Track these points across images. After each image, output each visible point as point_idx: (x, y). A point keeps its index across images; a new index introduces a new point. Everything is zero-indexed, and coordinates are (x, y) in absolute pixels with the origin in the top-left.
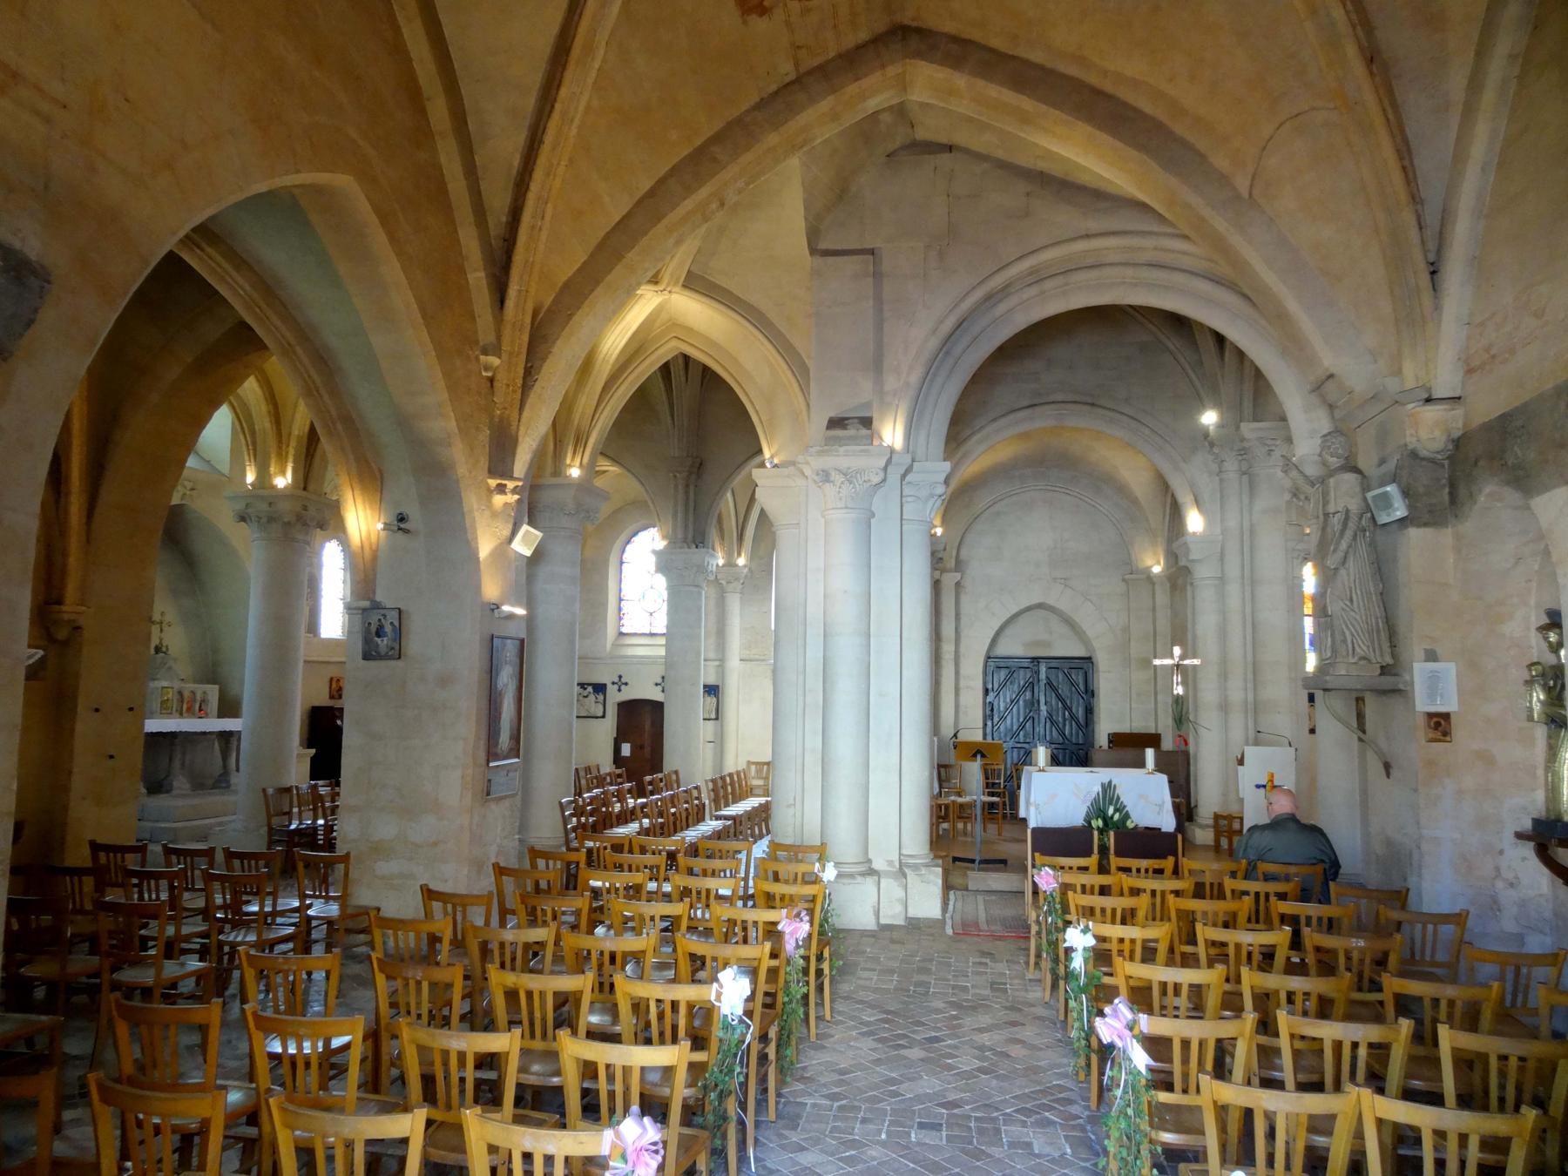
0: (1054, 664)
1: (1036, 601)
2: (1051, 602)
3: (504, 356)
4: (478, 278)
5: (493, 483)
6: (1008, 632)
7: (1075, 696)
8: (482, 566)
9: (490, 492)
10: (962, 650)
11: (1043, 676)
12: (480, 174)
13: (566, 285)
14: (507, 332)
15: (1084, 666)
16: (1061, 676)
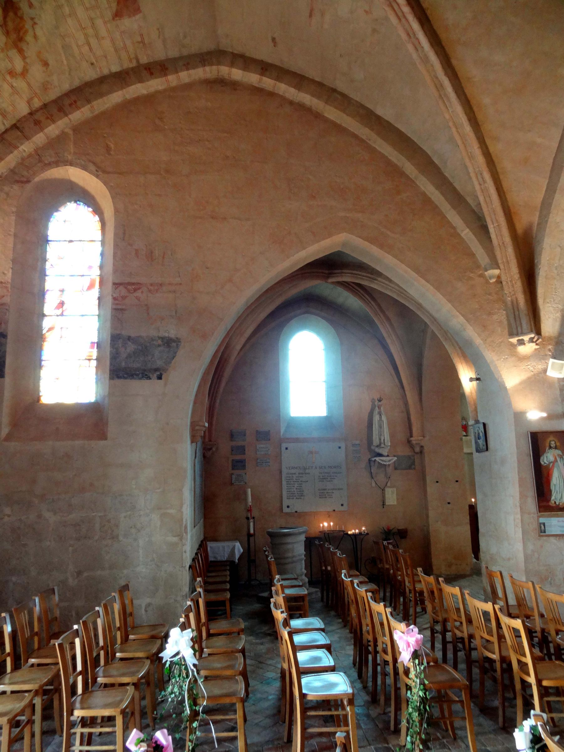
3: (502, 266)
4: (466, 234)
5: (514, 340)
8: (510, 392)
9: (513, 346)
12: (451, 180)
13: (543, 203)
14: (498, 253)
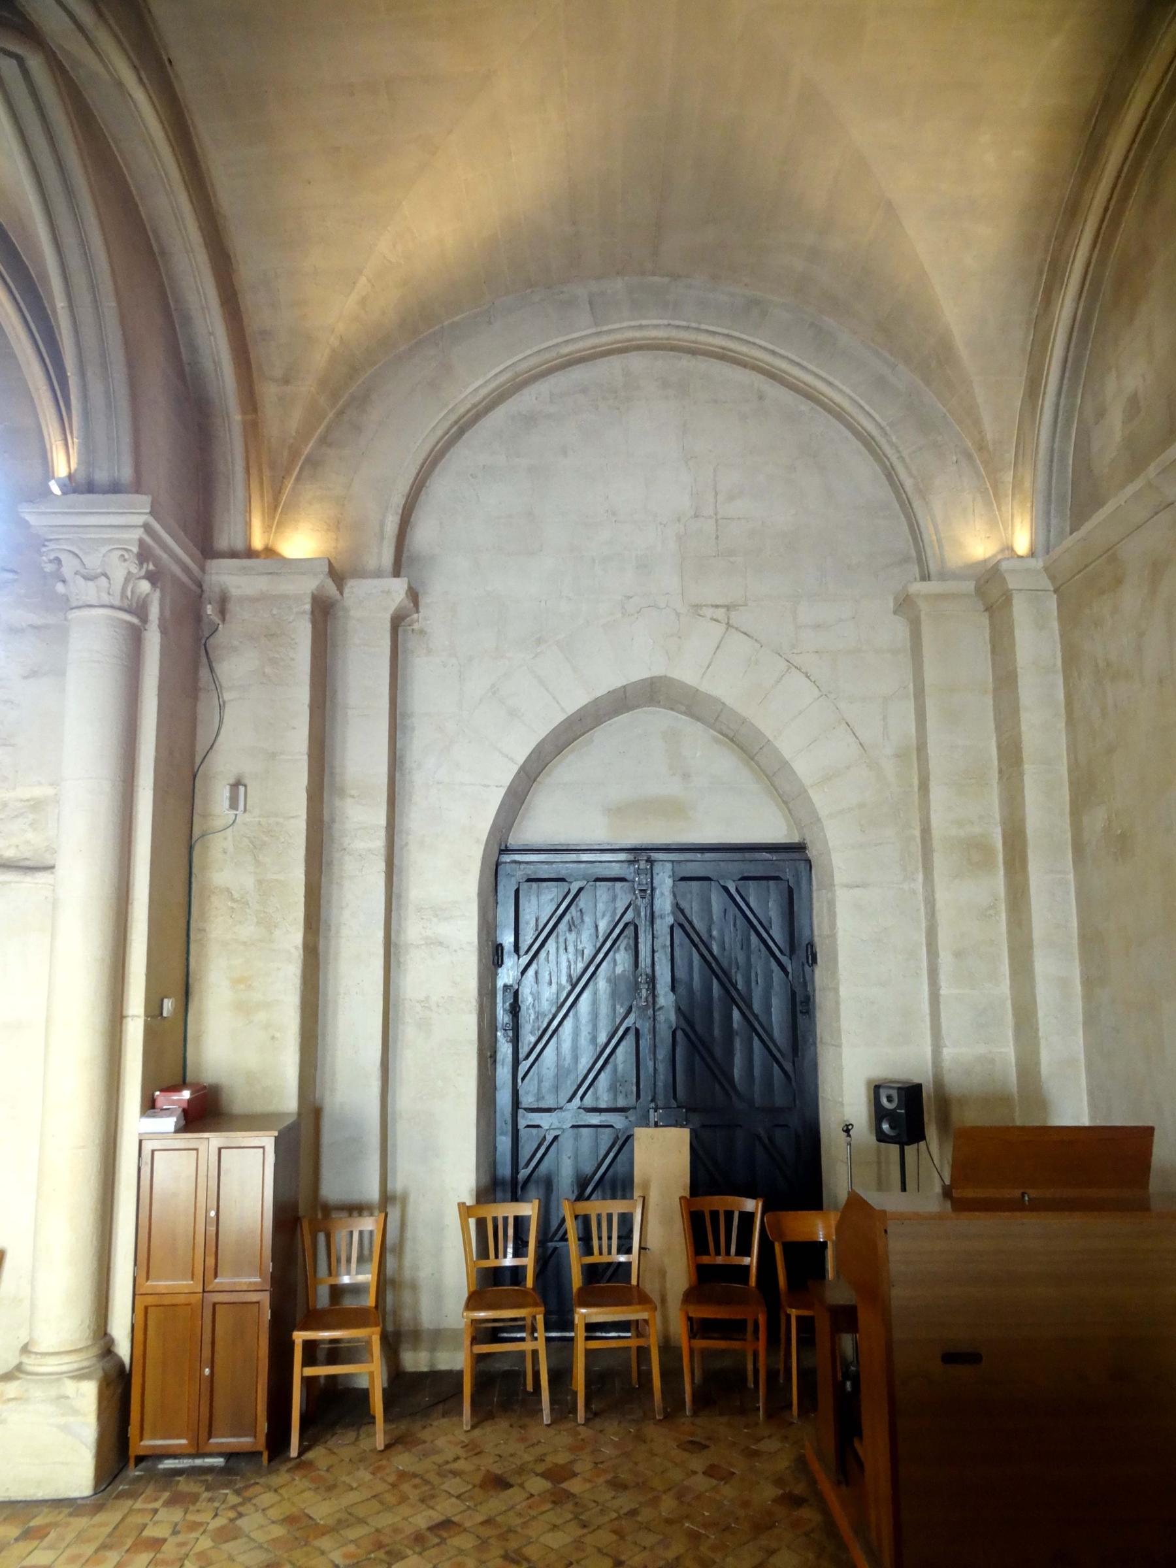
0: (696, 865)
1: (637, 672)
2: (687, 674)
6: (569, 770)
7: (759, 962)
10: (415, 820)
11: (664, 903)
15: (783, 871)
16: (717, 901)
